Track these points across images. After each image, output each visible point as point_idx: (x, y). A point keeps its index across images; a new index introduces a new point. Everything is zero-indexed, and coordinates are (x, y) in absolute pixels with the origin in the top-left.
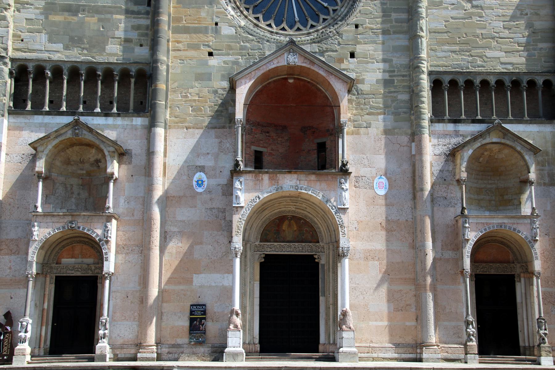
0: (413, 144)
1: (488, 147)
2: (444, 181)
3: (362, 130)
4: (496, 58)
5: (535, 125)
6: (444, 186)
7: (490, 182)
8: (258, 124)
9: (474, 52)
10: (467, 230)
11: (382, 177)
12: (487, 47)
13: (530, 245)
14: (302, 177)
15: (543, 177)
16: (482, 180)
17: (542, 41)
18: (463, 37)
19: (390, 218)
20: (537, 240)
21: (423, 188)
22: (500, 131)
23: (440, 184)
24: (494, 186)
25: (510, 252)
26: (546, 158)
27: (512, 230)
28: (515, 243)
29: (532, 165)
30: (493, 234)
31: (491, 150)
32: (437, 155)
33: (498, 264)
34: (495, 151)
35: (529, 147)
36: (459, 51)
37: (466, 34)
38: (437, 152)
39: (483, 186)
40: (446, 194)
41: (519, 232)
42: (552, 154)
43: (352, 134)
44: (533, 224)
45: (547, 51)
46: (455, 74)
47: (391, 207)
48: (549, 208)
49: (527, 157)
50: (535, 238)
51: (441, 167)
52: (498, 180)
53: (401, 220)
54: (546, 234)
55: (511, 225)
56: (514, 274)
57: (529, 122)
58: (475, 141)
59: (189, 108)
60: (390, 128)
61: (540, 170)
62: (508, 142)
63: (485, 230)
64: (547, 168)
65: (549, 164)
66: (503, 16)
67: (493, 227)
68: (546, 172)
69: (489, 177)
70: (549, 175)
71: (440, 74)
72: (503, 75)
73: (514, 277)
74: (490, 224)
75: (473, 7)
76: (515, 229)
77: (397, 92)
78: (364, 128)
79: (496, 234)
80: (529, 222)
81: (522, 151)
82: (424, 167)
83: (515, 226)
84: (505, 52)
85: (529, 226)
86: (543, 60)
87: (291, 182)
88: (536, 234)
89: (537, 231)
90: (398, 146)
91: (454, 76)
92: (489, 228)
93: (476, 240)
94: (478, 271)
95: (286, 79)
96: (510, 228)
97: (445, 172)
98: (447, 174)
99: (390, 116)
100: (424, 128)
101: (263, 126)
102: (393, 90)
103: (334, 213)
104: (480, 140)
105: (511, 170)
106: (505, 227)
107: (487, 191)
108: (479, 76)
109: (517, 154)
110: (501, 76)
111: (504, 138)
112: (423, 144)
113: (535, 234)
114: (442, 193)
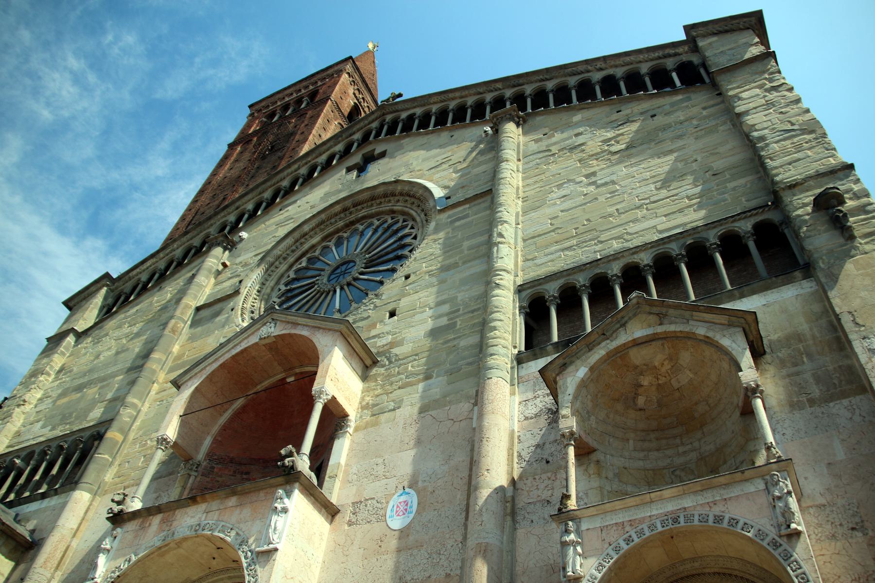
0: (476, 408)
1: (637, 356)
2: (546, 465)
3: (383, 418)
4: (649, 228)
5: (754, 296)
6: (544, 476)
7: (681, 449)
8: (232, 461)
9: (603, 237)
10: (571, 550)
11: (407, 490)
12: (629, 222)
13: (776, 553)
14: (215, 505)
15: (802, 388)
16: (658, 450)
17: (734, 178)
18: (584, 225)
19: (409, 578)
20: (798, 534)
21: (478, 483)
22: (650, 313)
23: (535, 474)
24: (694, 455)
26: (800, 346)
27: (711, 523)
29: (743, 354)
31: (649, 368)
32: (531, 418)
34: (663, 370)
35: (723, 319)
36: (577, 245)
37: (586, 220)
38: (532, 410)
39: (661, 464)
40: (550, 492)
41: (734, 522)
42: (814, 337)
43: (365, 428)
44: (771, 489)
45: (749, 186)
46: (569, 275)
47: (415, 552)
48: (840, 453)
49: (726, 342)
50: (789, 526)
51: (538, 438)
52: (699, 440)
53: (434, 577)
54: (853, 529)
55: (705, 510)
57: (736, 293)
58: (590, 350)
59: (140, 459)
60: (438, 397)
61: (789, 376)
62: (672, 328)
63: (628, 540)
64: (807, 365)
65: (810, 356)
66: (654, 176)
67: (652, 527)
68: (808, 376)
69: (678, 441)
70: (818, 380)
71: (540, 284)
72: (664, 243)
74: (642, 521)
75: (598, 187)
76: (719, 519)
77: (459, 337)
78: (389, 411)
79: (696, 564)
80: (762, 486)
81: (710, 334)
82: (484, 440)
83: (717, 510)
84: (665, 216)
85: (763, 500)
86: (743, 200)
87: (193, 520)
88: (787, 514)
89: (787, 505)
90: (449, 423)
91: (568, 278)
92: (641, 533)
93: (599, 576)
95: (284, 379)
96: (704, 519)
97: (547, 446)
98: (553, 449)
99: (440, 378)
100: (490, 368)
101: (240, 464)
102: (453, 337)
103: (245, 565)
104: (603, 344)
105: (720, 400)
106: (688, 519)
107: (678, 473)
108: (617, 262)
109: (708, 351)
110: (661, 247)
111: (661, 324)
112: (486, 397)
113: (783, 515)
114: (539, 493)
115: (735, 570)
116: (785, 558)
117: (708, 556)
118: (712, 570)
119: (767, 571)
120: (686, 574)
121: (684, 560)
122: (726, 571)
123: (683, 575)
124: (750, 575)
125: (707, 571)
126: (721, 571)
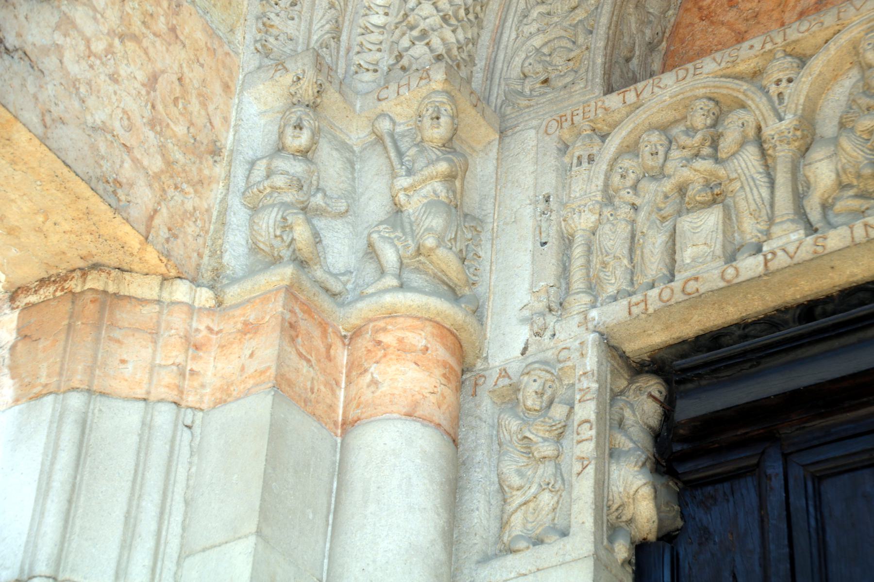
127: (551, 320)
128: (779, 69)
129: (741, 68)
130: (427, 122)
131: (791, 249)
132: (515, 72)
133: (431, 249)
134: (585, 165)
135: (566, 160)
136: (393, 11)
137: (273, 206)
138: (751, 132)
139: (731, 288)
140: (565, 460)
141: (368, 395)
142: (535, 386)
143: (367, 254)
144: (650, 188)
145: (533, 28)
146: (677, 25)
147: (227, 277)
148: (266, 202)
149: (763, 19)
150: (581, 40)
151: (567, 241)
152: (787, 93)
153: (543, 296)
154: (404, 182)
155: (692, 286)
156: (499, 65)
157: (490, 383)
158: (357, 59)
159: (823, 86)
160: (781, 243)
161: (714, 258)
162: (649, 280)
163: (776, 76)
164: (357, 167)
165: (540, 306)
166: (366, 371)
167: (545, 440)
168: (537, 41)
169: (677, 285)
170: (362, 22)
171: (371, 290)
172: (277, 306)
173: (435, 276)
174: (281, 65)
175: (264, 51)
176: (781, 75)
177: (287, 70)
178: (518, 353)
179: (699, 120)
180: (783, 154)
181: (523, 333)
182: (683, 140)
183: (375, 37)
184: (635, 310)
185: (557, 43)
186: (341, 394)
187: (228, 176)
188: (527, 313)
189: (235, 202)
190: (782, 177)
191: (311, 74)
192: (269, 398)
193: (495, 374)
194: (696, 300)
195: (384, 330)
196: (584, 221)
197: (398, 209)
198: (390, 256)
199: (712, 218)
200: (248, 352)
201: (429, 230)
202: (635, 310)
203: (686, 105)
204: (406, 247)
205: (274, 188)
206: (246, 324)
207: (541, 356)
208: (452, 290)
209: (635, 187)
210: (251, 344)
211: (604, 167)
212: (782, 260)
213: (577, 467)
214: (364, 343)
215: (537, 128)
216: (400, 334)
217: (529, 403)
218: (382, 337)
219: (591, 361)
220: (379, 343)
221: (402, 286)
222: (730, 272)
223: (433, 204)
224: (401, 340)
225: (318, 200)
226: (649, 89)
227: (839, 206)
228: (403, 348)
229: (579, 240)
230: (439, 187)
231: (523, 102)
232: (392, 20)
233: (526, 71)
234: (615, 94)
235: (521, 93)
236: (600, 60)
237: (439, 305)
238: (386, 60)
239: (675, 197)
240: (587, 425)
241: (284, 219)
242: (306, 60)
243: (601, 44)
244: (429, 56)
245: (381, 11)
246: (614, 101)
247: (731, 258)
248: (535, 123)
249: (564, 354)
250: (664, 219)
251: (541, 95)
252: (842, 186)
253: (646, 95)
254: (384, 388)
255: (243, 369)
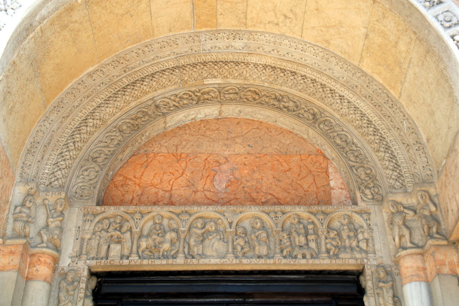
25: (329, 152)
28: (352, 89)
30: (221, 44)
33: (254, 211)
56: (360, 273)
73: (362, 291)
94: (116, 249)
115: (305, 66)
116: (447, 24)
117: (263, 33)
118: (263, 61)
119: (365, 74)
120: (214, 57)
121: (218, 31)
122: (289, 67)
123: (208, 58)
124: (330, 78)
125: (254, 59)
126: (278, 64)
127: (77, 259)
128: (138, 216)
129: (129, 211)
130: (59, 206)
131: (135, 261)
132: (74, 190)
133: (56, 239)
134: (90, 222)
135: (85, 218)
136: (50, 170)
137: (22, 221)
138: (129, 228)
139: (121, 265)
140: (76, 296)
141: (35, 273)
142: (71, 276)
143: (38, 234)
144: (104, 234)
145: (80, 181)
146: (109, 186)
147: (6, 236)
148: (19, 219)
149: (129, 193)
150: (92, 189)
151: (83, 239)
152: (138, 222)
153: (75, 252)
154: (51, 220)
155: (112, 262)
156: (70, 187)
157: (59, 271)
158: (40, 181)
159: (145, 223)
160: (133, 258)
161: (118, 257)
162: (101, 256)
163: (137, 217)
164: (37, 209)
165: (75, 255)
166: (35, 266)
167: (72, 290)
168: (81, 184)
169: (109, 261)
170: (43, 171)
171: (40, 246)
172: (21, 249)
173: (54, 244)
174: (27, 183)
175: (21, 177)
176: (138, 217)
177: (29, 185)
178: (67, 265)
179: (118, 221)
180: (136, 237)
181: (69, 261)
182: (114, 224)
183: (45, 176)
184: (98, 264)
185: (86, 187)
186: (27, 269)
187: (10, 208)
188: (71, 255)
189: (11, 216)
190: (135, 243)
191: (35, 189)
192: (16, 273)
193: (60, 269)
194: (112, 265)
195: (41, 257)
196: (88, 236)
197: (47, 226)
198: (45, 238)
199: (118, 247)
200: (11, 259)
201: (56, 234)
202: (98, 264)
203: (115, 216)
204: (49, 236)
205: (22, 216)
206: (11, 251)
207: (73, 268)
208: (56, 248)
209: (100, 231)
210: (12, 257)
211: (94, 224)
212: (133, 263)
213: (79, 299)
214: (35, 259)
215: (79, 208)
216: (45, 259)
217: (69, 280)
218: (40, 258)
219: (86, 273)
220: (40, 260)
221: (47, 247)
222: (121, 262)
223: (57, 227)
224: (45, 260)
225: (30, 219)
226: (107, 209)
227: (145, 252)
228: (45, 263)
229: (86, 241)
230: (59, 223)
231: (75, 200)
232: (50, 172)
233: (77, 191)
234: (99, 207)
235: (75, 197)
236: (96, 196)
237: (54, 253)
238: (47, 183)
239: (110, 238)
240: (82, 289)
241: (25, 226)
242: (35, 185)
243: (97, 192)
244: (58, 185)
245: (48, 169)
246: (98, 208)
247: (121, 258)
248: (78, 206)
249: (79, 269)
250: (107, 243)
251: (80, 199)
252: (147, 248)
253: (106, 210)
254: (40, 272)
255: (9, 263)
